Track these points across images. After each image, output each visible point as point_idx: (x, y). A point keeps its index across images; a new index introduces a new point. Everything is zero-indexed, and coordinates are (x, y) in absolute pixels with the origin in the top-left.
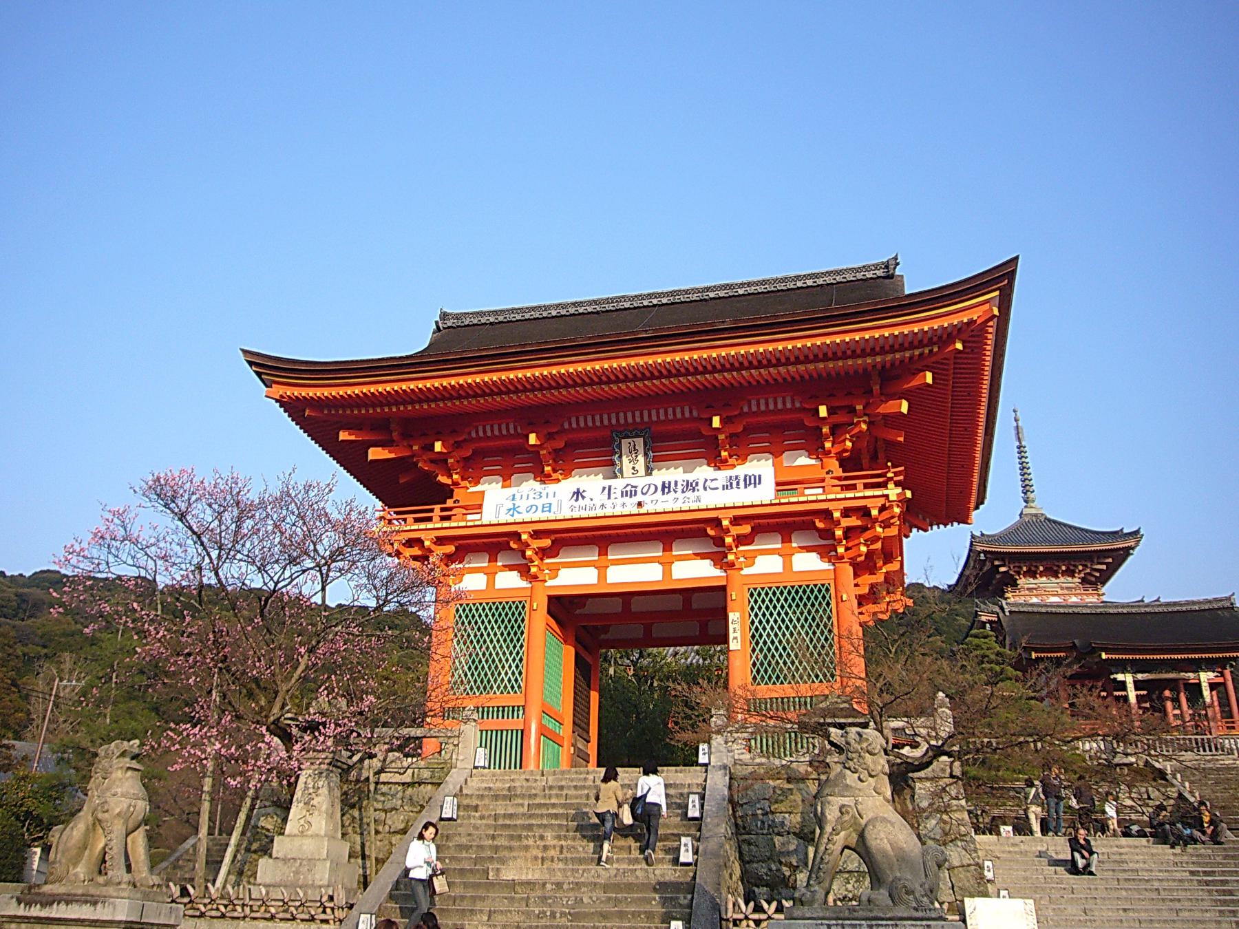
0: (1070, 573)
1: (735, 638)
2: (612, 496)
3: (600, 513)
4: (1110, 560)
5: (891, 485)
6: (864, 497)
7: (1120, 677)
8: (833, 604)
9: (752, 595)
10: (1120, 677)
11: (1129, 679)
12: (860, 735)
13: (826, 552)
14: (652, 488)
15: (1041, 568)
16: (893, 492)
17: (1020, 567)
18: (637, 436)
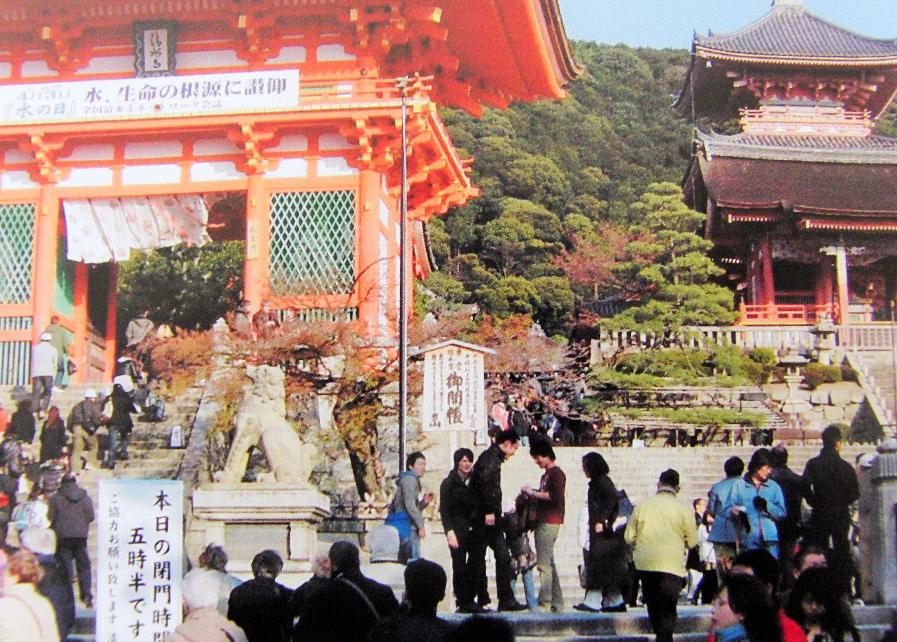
0: (832, 92)
1: (254, 247)
2: (130, 98)
3: (115, 116)
4: (882, 79)
5: (417, 96)
6: (389, 108)
7: (830, 251)
8: (356, 211)
9: (274, 201)
10: (830, 251)
11: (840, 255)
12: (265, 371)
13: (353, 156)
14: (172, 91)
15: (791, 86)
16: (419, 102)
17: (764, 83)
18: (161, 27)
